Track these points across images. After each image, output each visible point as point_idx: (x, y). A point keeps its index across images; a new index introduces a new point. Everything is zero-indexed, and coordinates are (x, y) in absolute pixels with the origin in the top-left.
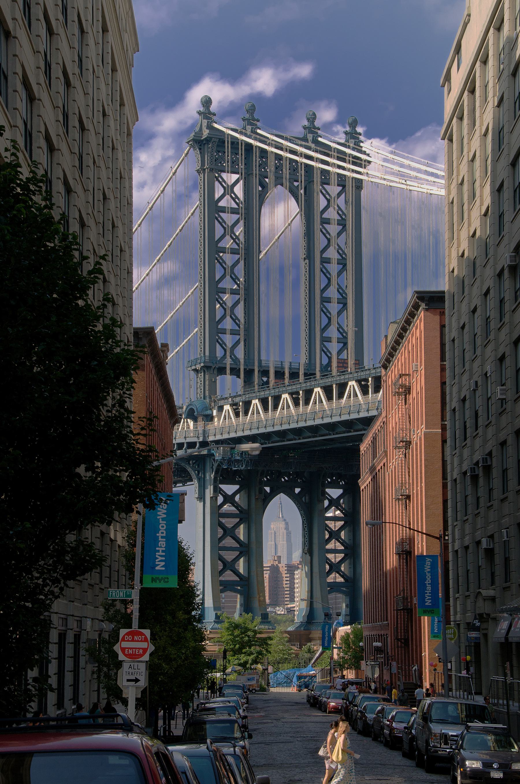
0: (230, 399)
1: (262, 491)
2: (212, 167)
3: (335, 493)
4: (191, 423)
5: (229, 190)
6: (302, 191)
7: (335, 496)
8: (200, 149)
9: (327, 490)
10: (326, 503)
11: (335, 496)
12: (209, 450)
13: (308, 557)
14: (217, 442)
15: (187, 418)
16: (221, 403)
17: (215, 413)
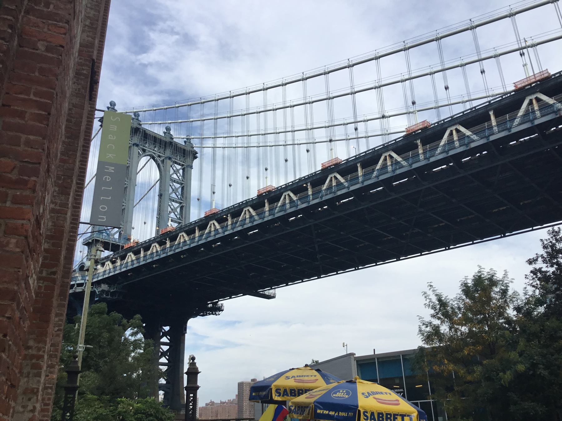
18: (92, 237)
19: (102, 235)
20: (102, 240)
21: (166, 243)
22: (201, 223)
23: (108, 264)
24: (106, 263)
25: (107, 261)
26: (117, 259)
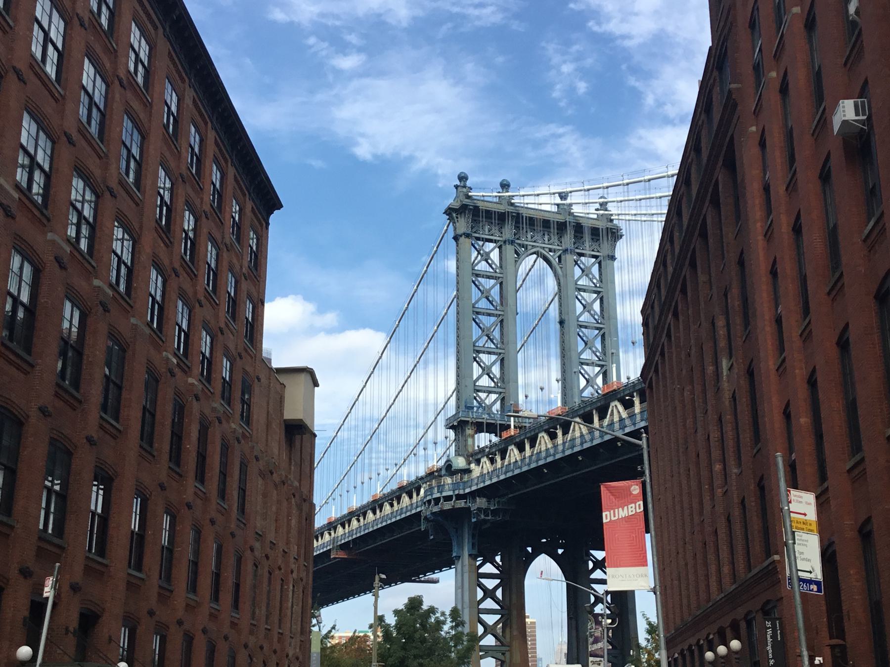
2: (469, 232)
4: (449, 480)
5: (486, 258)
6: (557, 259)
8: (457, 218)
13: (574, 622)
16: (479, 456)
17: (473, 466)
18: (456, 417)
19: (472, 412)
20: (473, 419)
21: (556, 433)
22: (599, 404)
23: (485, 462)
24: (483, 460)
25: (483, 457)
26: (496, 455)
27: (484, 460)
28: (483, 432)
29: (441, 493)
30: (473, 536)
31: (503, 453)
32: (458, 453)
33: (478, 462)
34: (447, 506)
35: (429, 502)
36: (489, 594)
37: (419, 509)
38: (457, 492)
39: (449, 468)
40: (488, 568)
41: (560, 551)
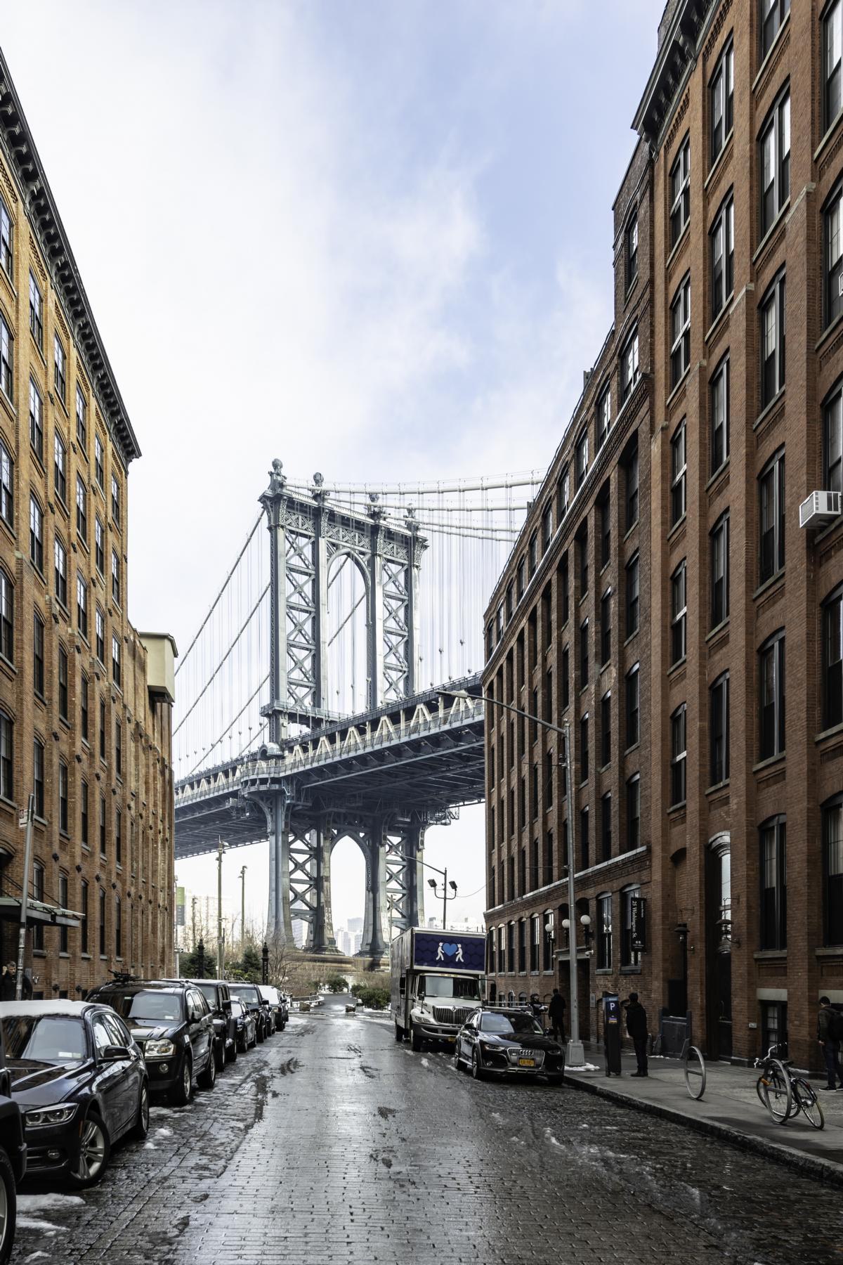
0: (300, 739)
1: (329, 830)
3: (395, 840)
4: (264, 764)
7: (395, 843)
9: (388, 837)
10: (387, 848)
11: (395, 843)
12: (280, 787)
14: (286, 778)
15: (260, 759)
16: (292, 744)
17: (286, 753)
27: (297, 748)
28: (296, 722)
29: (258, 774)
30: (286, 816)
31: (316, 743)
32: (271, 740)
33: (291, 750)
34: (263, 788)
35: (246, 782)
36: (299, 866)
37: (236, 788)
38: (272, 775)
39: (264, 754)
40: (299, 845)
41: (362, 835)
